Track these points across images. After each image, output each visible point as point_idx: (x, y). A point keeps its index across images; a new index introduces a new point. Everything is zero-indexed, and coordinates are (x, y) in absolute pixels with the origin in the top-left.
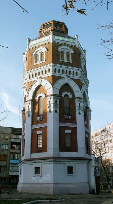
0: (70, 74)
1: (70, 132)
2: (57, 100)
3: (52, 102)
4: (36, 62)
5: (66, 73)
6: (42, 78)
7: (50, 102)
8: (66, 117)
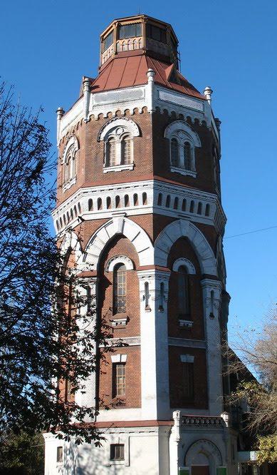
0: (191, 211)
1: (191, 359)
2: (164, 282)
3: (152, 286)
4: (108, 165)
6: (126, 216)
7: (147, 284)
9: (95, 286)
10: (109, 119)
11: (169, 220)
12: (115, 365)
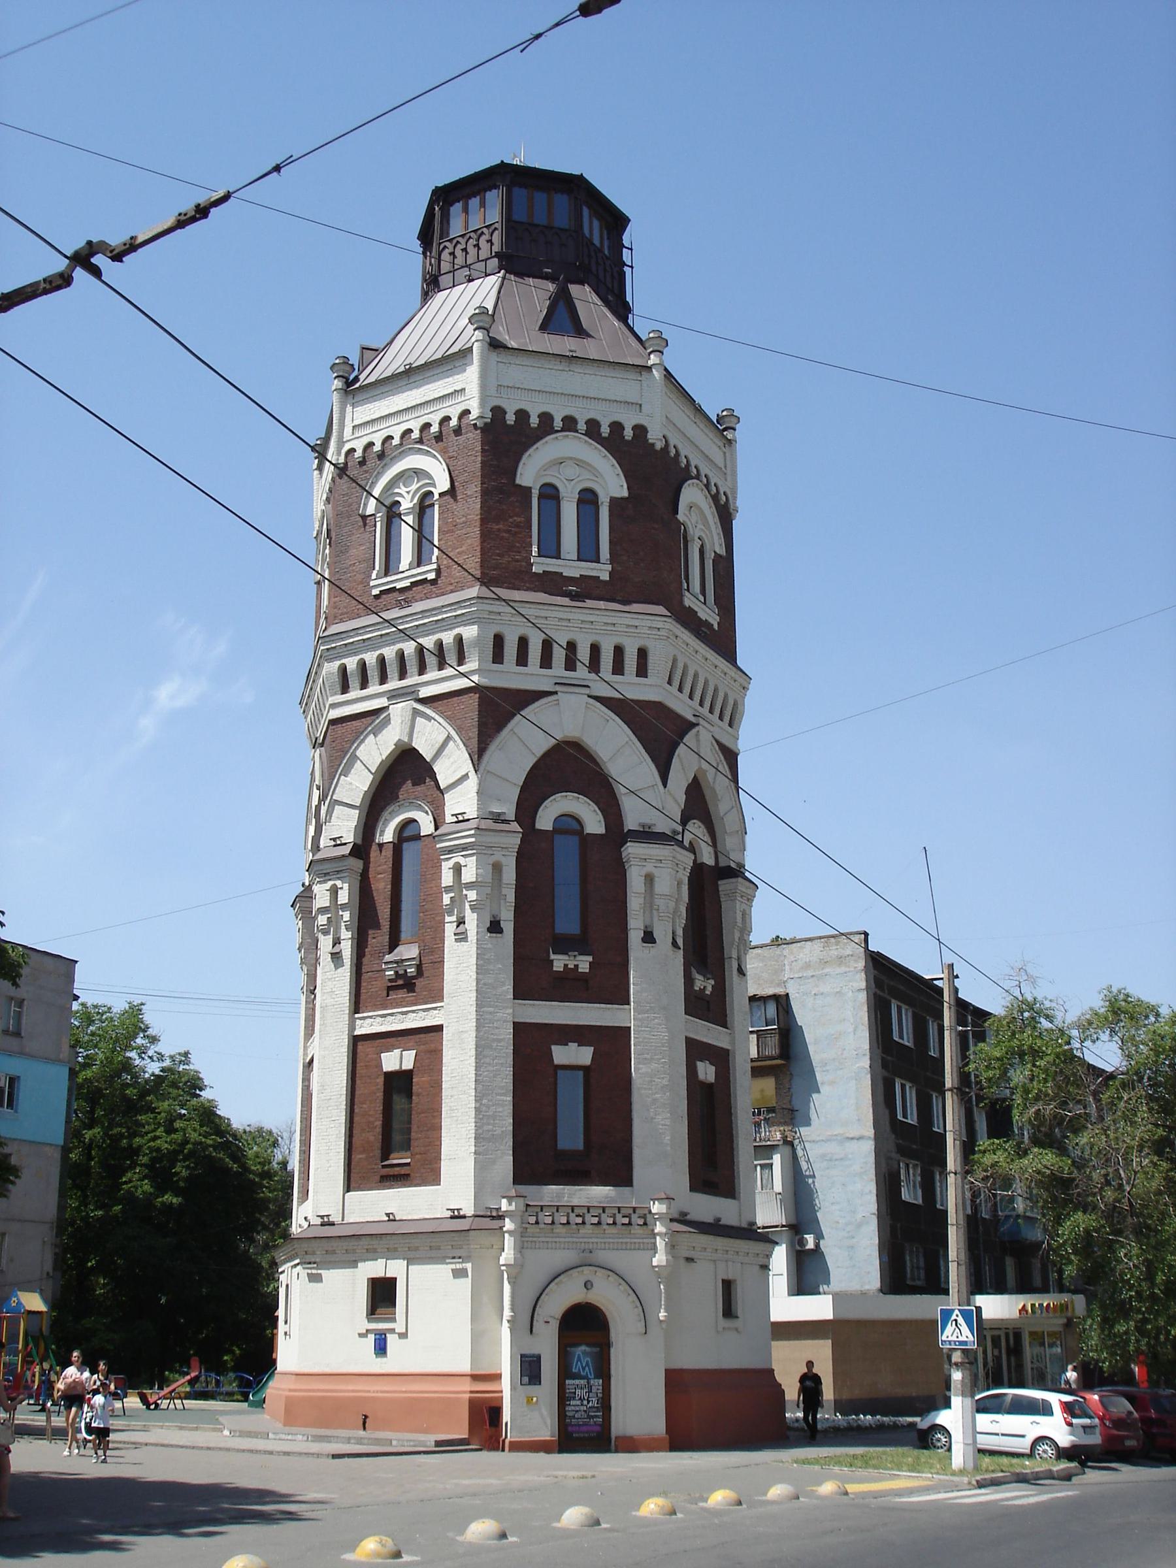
1: (583, 1055)
2: (503, 860)
5: (570, 665)
8: (559, 962)
9: (346, 886)
10: (385, 455)
11: (526, 698)
12: (389, 1076)
